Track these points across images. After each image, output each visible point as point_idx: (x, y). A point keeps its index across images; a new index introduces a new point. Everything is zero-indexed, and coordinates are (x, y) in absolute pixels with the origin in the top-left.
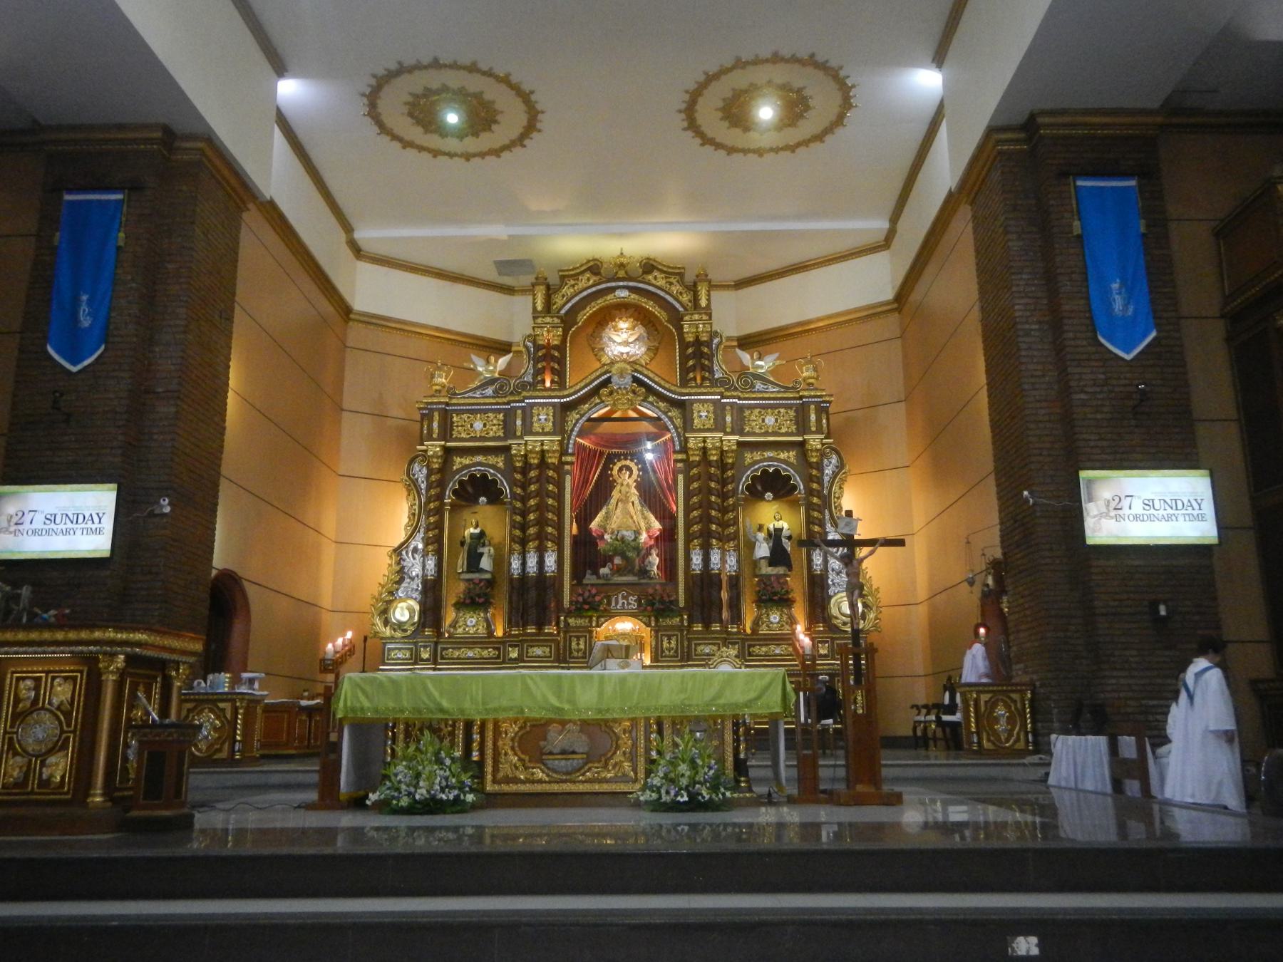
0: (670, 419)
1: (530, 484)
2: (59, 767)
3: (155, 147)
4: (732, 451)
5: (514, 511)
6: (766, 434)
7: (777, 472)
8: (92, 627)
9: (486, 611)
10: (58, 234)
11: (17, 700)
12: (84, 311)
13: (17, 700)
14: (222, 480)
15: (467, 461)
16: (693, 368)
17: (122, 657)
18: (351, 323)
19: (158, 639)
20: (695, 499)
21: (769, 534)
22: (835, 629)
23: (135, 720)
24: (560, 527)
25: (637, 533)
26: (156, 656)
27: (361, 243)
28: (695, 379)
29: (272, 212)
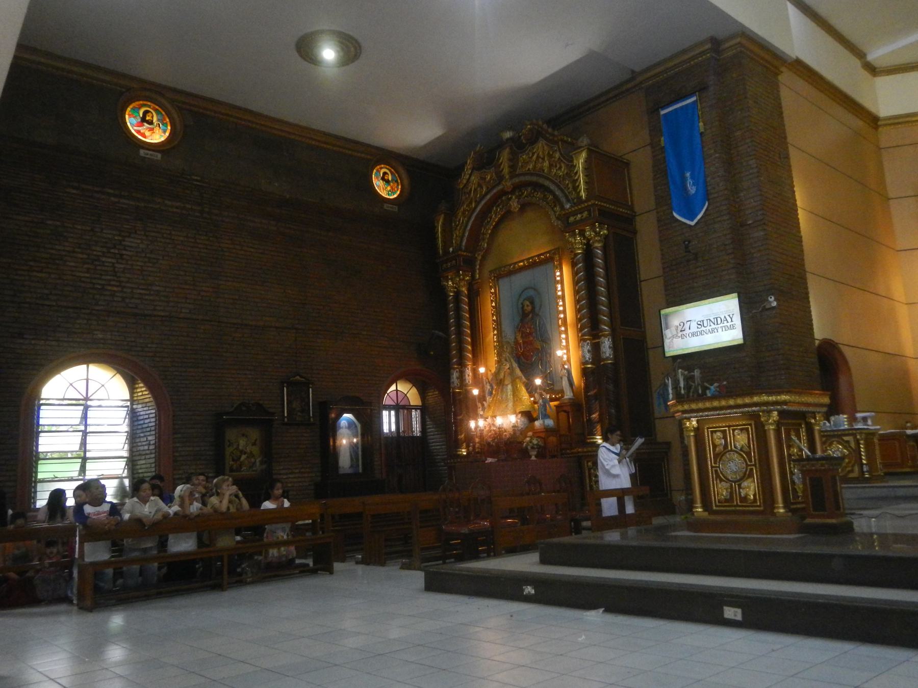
2: (750, 489)
3: (708, 55)
8: (751, 394)
10: (662, 139)
12: (690, 183)
13: (715, 446)
14: (809, 276)
17: (775, 413)
18: (880, 129)
19: (797, 397)
23: (794, 455)
26: (798, 410)
27: (876, 64)
29: (800, 68)
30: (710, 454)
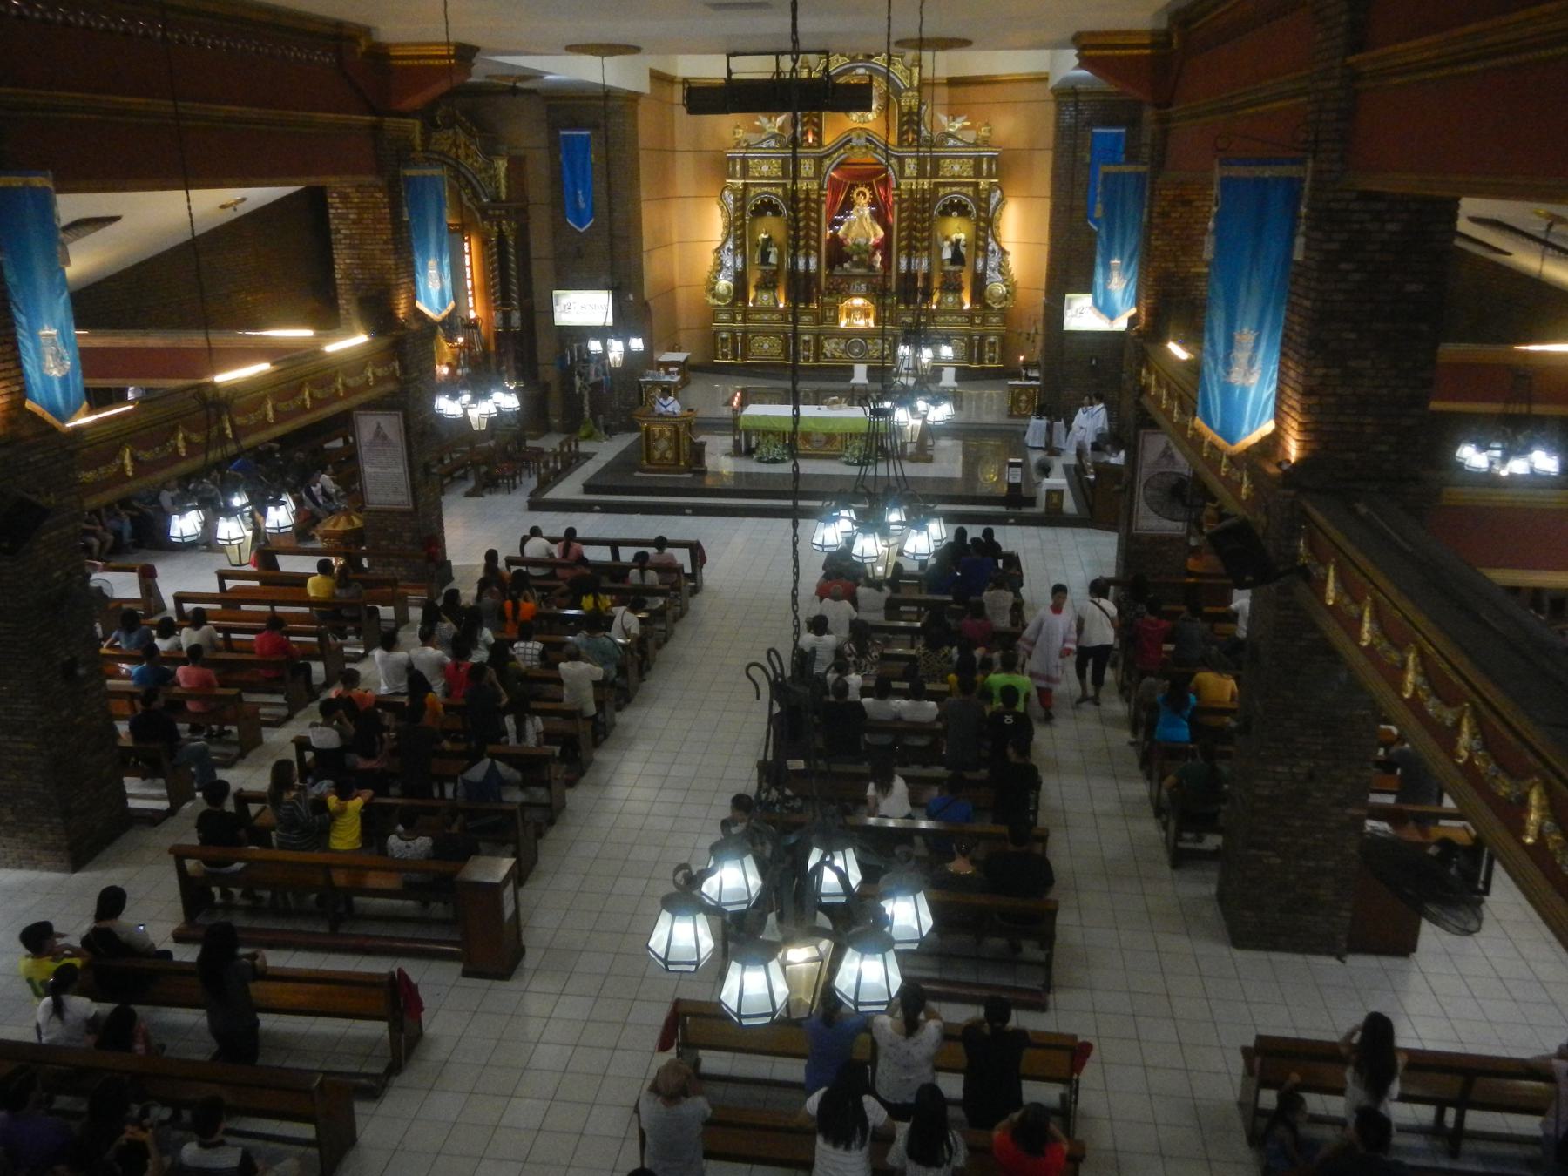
2: (669, 455)
6: (953, 177)
7: (959, 202)
9: (774, 291)
11: (654, 435)
15: (759, 190)
16: (907, 132)
20: (904, 224)
21: (952, 244)
22: (986, 306)
24: (818, 240)
25: (868, 239)
28: (908, 139)
30: (651, 437)
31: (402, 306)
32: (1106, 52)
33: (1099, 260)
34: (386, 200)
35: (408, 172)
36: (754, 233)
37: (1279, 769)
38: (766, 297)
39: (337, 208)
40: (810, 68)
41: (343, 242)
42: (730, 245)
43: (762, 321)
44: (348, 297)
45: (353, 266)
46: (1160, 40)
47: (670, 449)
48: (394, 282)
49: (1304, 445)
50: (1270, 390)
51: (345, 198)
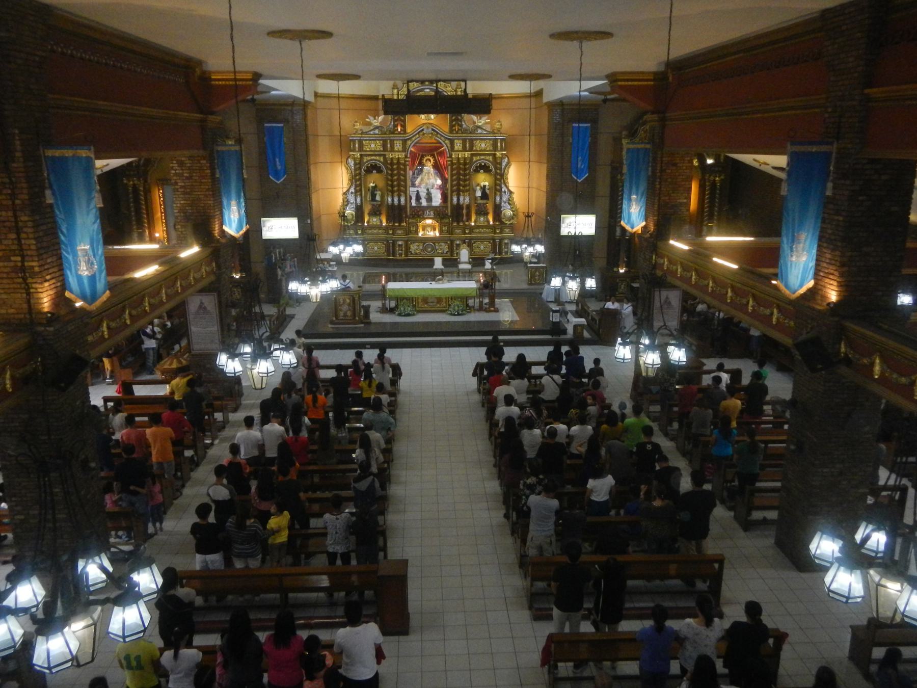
0: (446, 144)
1: (394, 170)
2: (349, 313)
4: (468, 157)
5: (388, 179)
7: (485, 164)
9: (380, 216)
15: (369, 158)
16: (454, 126)
20: (455, 177)
21: (481, 188)
22: (502, 223)
31: (217, 228)
32: (630, 83)
33: (625, 196)
34: (208, 165)
35: (219, 148)
36: (365, 182)
37: (825, 470)
38: (375, 219)
39: (176, 170)
40: (397, 88)
41: (180, 190)
42: (352, 190)
43: (372, 234)
44: (182, 224)
45: (184, 205)
46: (660, 77)
47: (350, 310)
48: (211, 214)
49: (840, 293)
50: (812, 264)
51: (181, 164)
